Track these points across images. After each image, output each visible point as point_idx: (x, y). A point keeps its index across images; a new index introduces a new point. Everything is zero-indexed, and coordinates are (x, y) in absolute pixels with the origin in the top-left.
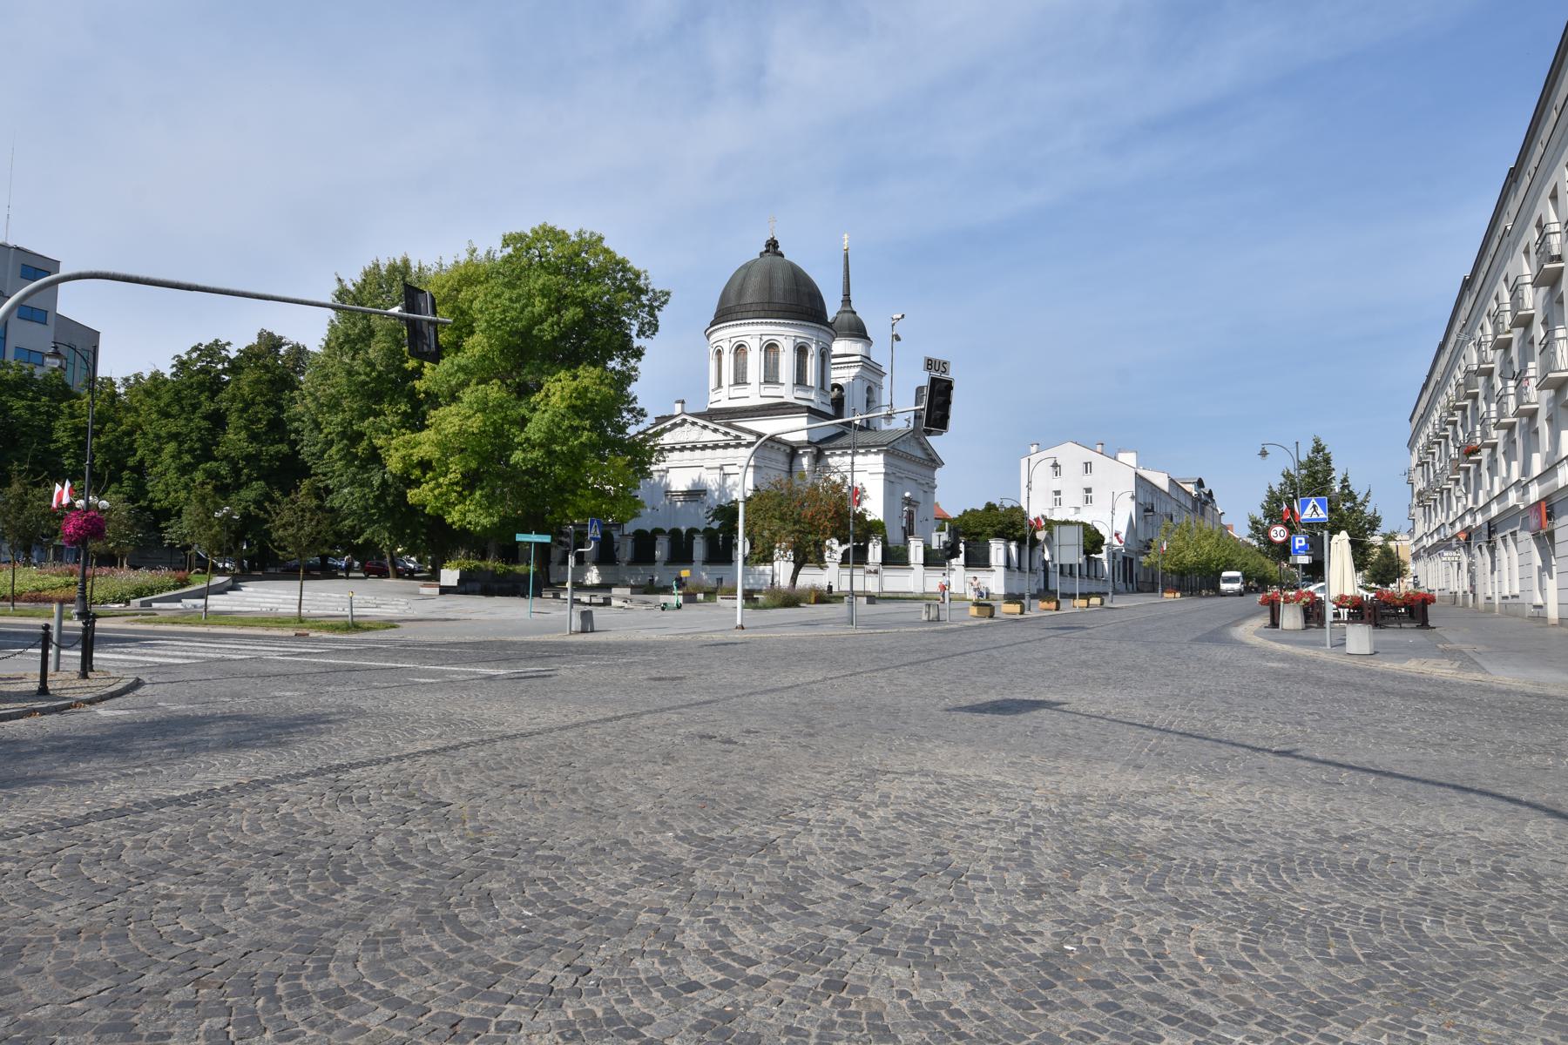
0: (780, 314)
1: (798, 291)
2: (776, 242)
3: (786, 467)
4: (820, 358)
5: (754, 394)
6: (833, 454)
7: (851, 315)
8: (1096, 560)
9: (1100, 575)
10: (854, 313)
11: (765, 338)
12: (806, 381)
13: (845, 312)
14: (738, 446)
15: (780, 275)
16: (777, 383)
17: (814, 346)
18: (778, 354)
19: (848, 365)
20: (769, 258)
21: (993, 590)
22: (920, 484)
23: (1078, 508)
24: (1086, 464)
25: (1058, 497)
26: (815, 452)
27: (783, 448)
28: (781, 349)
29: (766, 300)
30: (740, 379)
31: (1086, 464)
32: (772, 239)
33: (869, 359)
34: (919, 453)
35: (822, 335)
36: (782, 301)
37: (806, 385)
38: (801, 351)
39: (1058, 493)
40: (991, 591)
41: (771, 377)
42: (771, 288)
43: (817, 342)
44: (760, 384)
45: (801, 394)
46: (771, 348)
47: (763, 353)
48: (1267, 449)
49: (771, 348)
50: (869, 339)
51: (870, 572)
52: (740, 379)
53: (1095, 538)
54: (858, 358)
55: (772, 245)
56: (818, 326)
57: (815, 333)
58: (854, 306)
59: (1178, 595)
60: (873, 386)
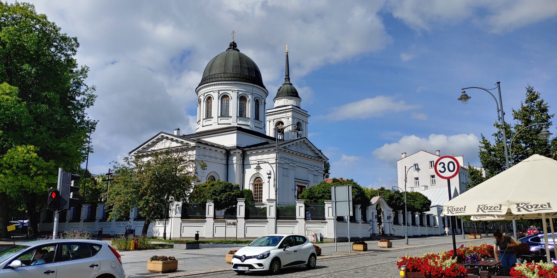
0: (230, 79)
1: (241, 66)
2: (235, 44)
3: (224, 162)
4: (254, 103)
5: (214, 124)
6: (252, 155)
7: (289, 85)
8: (428, 216)
9: (432, 223)
10: (291, 84)
11: (221, 92)
12: (245, 115)
13: (286, 84)
14: (187, 149)
15: (232, 58)
16: (228, 116)
17: (250, 96)
18: (228, 101)
19: (286, 111)
20: (232, 52)
21: (325, 235)
22: (310, 170)
23: (427, 186)
24: (431, 162)
25: (417, 181)
26: (241, 152)
27: (219, 150)
28: (230, 98)
29: (223, 72)
30: (209, 116)
31: (431, 162)
32: (233, 42)
33: (299, 108)
34: (310, 153)
35: (255, 89)
36: (231, 72)
37: (245, 117)
38: (242, 99)
39: (417, 179)
40: (324, 237)
41: (224, 114)
42: (225, 65)
43: (252, 94)
44: (218, 117)
45: (241, 122)
46: (224, 97)
47: (220, 100)
48: (468, 92)
49: (224, 97)
50: (299, 98)
51: (230, 224)
52: (209, 116)
53: (422, 201)
54: (291, 107)
55: (233, 46)
56: (253, 85)
57: (251, 88)
58: (291, 81)
59: (478, 236)
60: (301, 122)
